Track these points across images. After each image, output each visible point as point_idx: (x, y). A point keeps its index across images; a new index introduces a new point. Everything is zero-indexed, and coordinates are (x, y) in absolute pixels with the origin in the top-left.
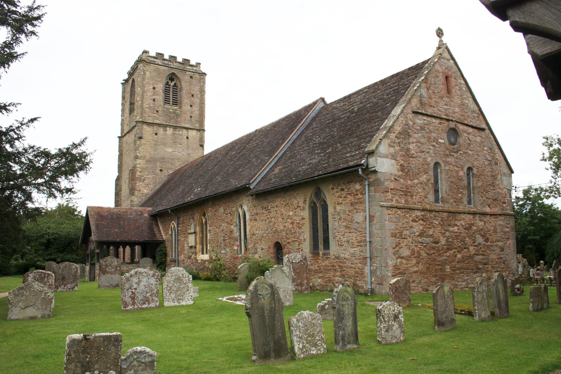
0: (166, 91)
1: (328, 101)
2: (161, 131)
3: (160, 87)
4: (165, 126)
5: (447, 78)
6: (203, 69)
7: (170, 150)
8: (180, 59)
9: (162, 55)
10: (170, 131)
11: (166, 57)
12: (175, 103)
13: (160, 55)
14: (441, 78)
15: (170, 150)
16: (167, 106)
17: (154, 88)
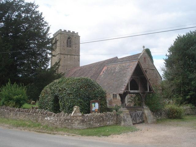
0: (67, 44)
1: (119, 58)
2: (66, 56)
3: (66, 41)
4: (67, 55)
5: (145, 58)
6: (79, 34)
7: (69, 62)
8: (71, 32)
9: (66, 31)
10: (69, 56)
11: (67, 31)
12: (70, 47)
13: (65, 31)
14: (143, 59)
15: (69, 62)
16: (68, 48)
17: (64, 42)
